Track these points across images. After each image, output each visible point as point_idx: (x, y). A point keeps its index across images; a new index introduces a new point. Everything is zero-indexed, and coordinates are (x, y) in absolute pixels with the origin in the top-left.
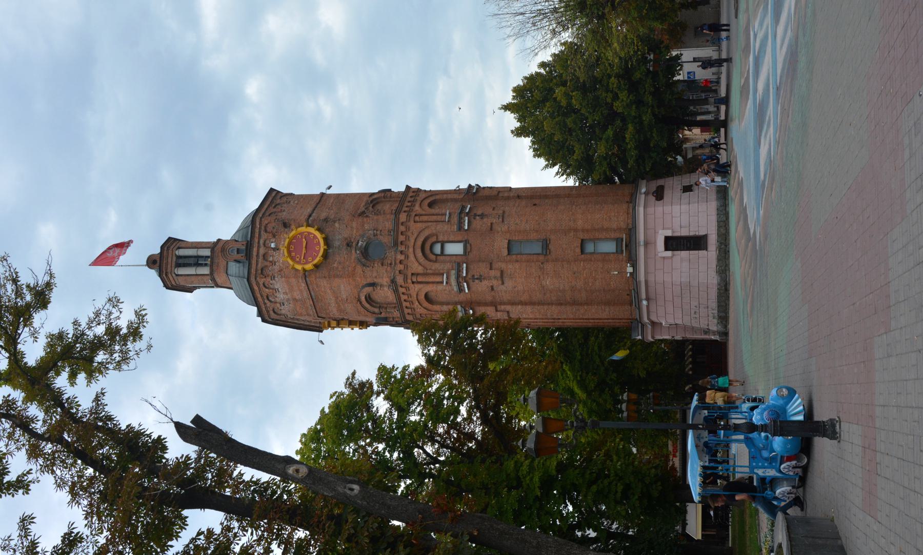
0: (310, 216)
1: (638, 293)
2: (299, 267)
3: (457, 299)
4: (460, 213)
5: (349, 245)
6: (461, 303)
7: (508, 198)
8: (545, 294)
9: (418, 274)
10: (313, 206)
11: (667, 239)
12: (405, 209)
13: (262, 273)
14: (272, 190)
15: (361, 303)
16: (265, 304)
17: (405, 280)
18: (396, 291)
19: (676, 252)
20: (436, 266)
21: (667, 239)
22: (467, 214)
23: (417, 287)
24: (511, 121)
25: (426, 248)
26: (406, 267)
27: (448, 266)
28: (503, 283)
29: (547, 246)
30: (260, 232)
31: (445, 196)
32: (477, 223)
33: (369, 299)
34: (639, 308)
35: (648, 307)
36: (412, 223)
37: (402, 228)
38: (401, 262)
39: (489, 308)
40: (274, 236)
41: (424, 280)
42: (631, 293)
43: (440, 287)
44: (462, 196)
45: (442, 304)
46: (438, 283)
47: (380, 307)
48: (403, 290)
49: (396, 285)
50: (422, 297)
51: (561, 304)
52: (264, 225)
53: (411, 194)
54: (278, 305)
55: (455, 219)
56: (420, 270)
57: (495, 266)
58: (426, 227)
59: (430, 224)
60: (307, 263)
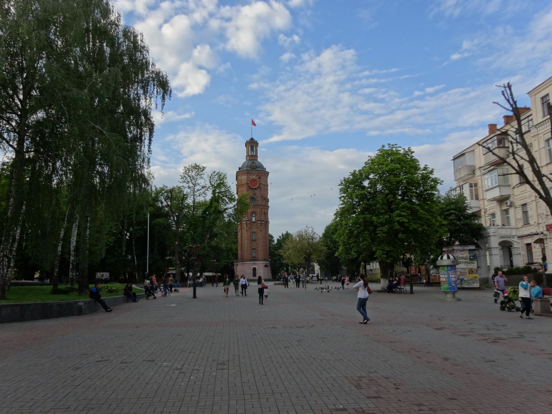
24: (284, 233)
25: (254, 212)
32: (259, 225)
42: (243, 260)
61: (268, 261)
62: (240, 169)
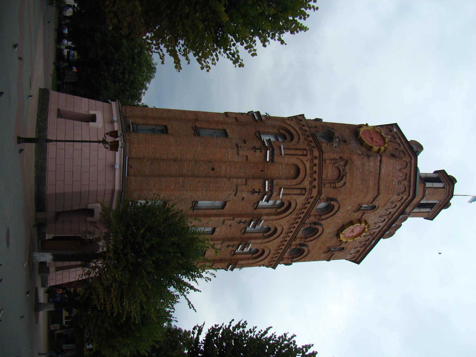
0: (381, 161)
5: (345, 141)
12: (316, 161)
22: (267, 149)
38: (304, 126)
40: (396, 149)
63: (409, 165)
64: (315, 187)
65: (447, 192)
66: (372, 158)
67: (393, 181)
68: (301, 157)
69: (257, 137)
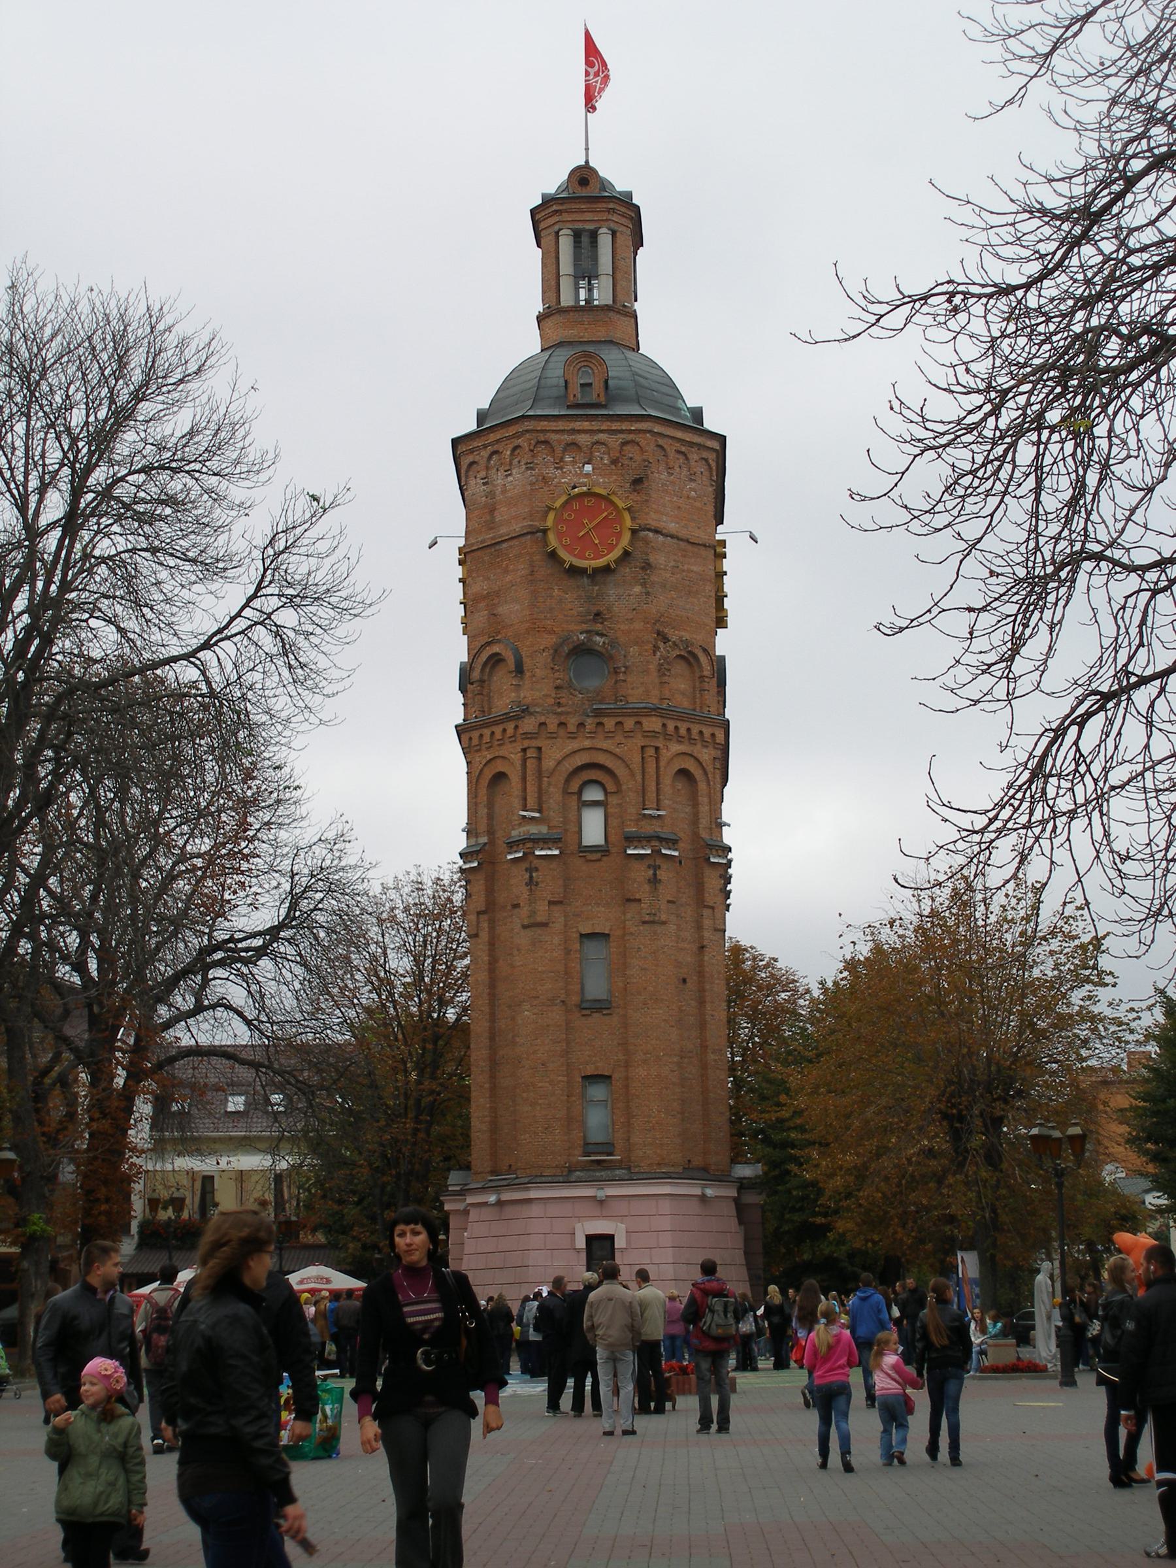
0: (657, 531)
1: (509, 1186)
2: (550, 522)
3: (499, 834)
4: (660, 839)
6: (492, 842)
7: (699, 927)
8: (509, 1007)
9: (539, 759)
10: (683, 533)
11: (610, 1238)
13: (538, 442)
14: (722, 439)
15: (488, 644)
16: (485, 447)
17: (527, 736)
18: (507, 718)
19: (584, 1256)
20: (554, 795)
21: (610, 1238)
23: (516, 758)
25: (594, 771)
26: (553, 736)
27: (557, 819)
28: (525, 927)
29: (599, 1010)
30: (621, 431)
31: (703, 800)
32: (641, 873)
33: (496, 660)
34: (484, 1189)
35: (485, 1204)
36: (639, 741)
37: (629, 723)
38: (562, 724)
39: (482, 898)
40: (614, 462)
41: (529, 772)
42: (507, 1174)
43: (516, 802)
44: (704, 834)
45: (490, 805)
46: (525, 799)
47: (482, 681)
48: (510, 731)
49: (517, 718)
50: (500, 767)
51: (492, 1038)
52: (637, 438)
53: (707, 731)
54: (483, 474)
55: (648, 828)
56: (548, 764)
57: (557, 911)
58: (633, 775)
59: (639, 777)
60: (560, 535)
61: (722, 1178)
62: (482, 416)
63: (661, 442)
64: (713, 735)
65: (623, 221)
66: (651, 559)
67: (688, 497)
68: (662, 764)
69: (599, 860)
